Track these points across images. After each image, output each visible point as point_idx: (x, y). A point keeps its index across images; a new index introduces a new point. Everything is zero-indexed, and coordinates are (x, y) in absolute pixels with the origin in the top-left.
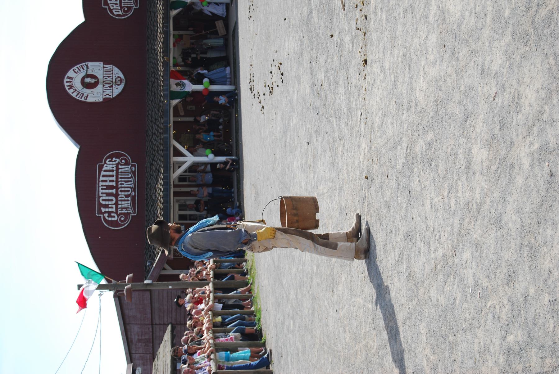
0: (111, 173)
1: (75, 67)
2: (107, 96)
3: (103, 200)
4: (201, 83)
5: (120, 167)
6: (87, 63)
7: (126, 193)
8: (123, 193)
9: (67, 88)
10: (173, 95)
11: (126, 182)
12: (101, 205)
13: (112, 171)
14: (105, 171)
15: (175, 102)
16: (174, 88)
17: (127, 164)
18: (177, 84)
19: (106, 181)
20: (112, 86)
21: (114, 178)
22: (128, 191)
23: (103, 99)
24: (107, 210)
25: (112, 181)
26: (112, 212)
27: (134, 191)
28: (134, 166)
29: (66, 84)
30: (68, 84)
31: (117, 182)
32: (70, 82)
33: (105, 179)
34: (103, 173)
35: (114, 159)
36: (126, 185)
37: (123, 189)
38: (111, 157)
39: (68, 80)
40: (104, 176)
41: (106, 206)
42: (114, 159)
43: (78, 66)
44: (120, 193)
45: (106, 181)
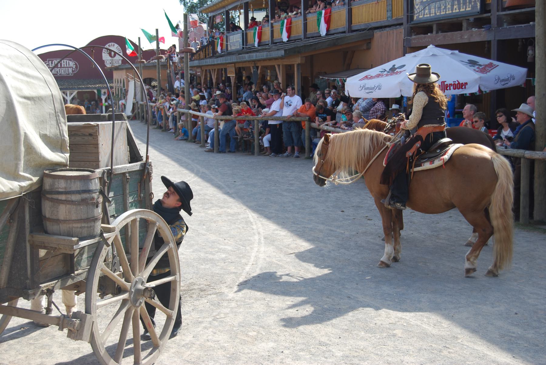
0: (68, 64)
1: (119, 47)
2: (105, 62)
3: (55, 62)
4: (105, 102)
5: (71, 68)
6: (122, 52)
7: (58, 72)
8: (58, 70)
9: (109, 44)
10: (99, 91)
11: (64, 71)
12: (52, 61)
13: (69, 65)
14: (69, 62)
15: (96, 91)
16: (103, 91)
17: (73, 71)
18: (105, 93)
19: (64, 63)
20: (110, 63)
21: (65, 66)
22: (60, 72)
23: (104, 60)
24: (50, 64)
25: (64, 65)
26: (49, 66)
27: (60, 75)
28: (72, 74)
29: (110, 44)
30: (111, 45)
31: (64, 67)
32: (112, 45)
33: (65, 62)
34: (68, 61)
35: (75, 66)
36: (63, 71)
37: (60, 70)
38: (76, 64)
39: (113, 45)
40: (66, 62)
41: (52, 63)
42: (75, 66)
43: (120, 49)
44: (58, 69)
45: (64, 63)
